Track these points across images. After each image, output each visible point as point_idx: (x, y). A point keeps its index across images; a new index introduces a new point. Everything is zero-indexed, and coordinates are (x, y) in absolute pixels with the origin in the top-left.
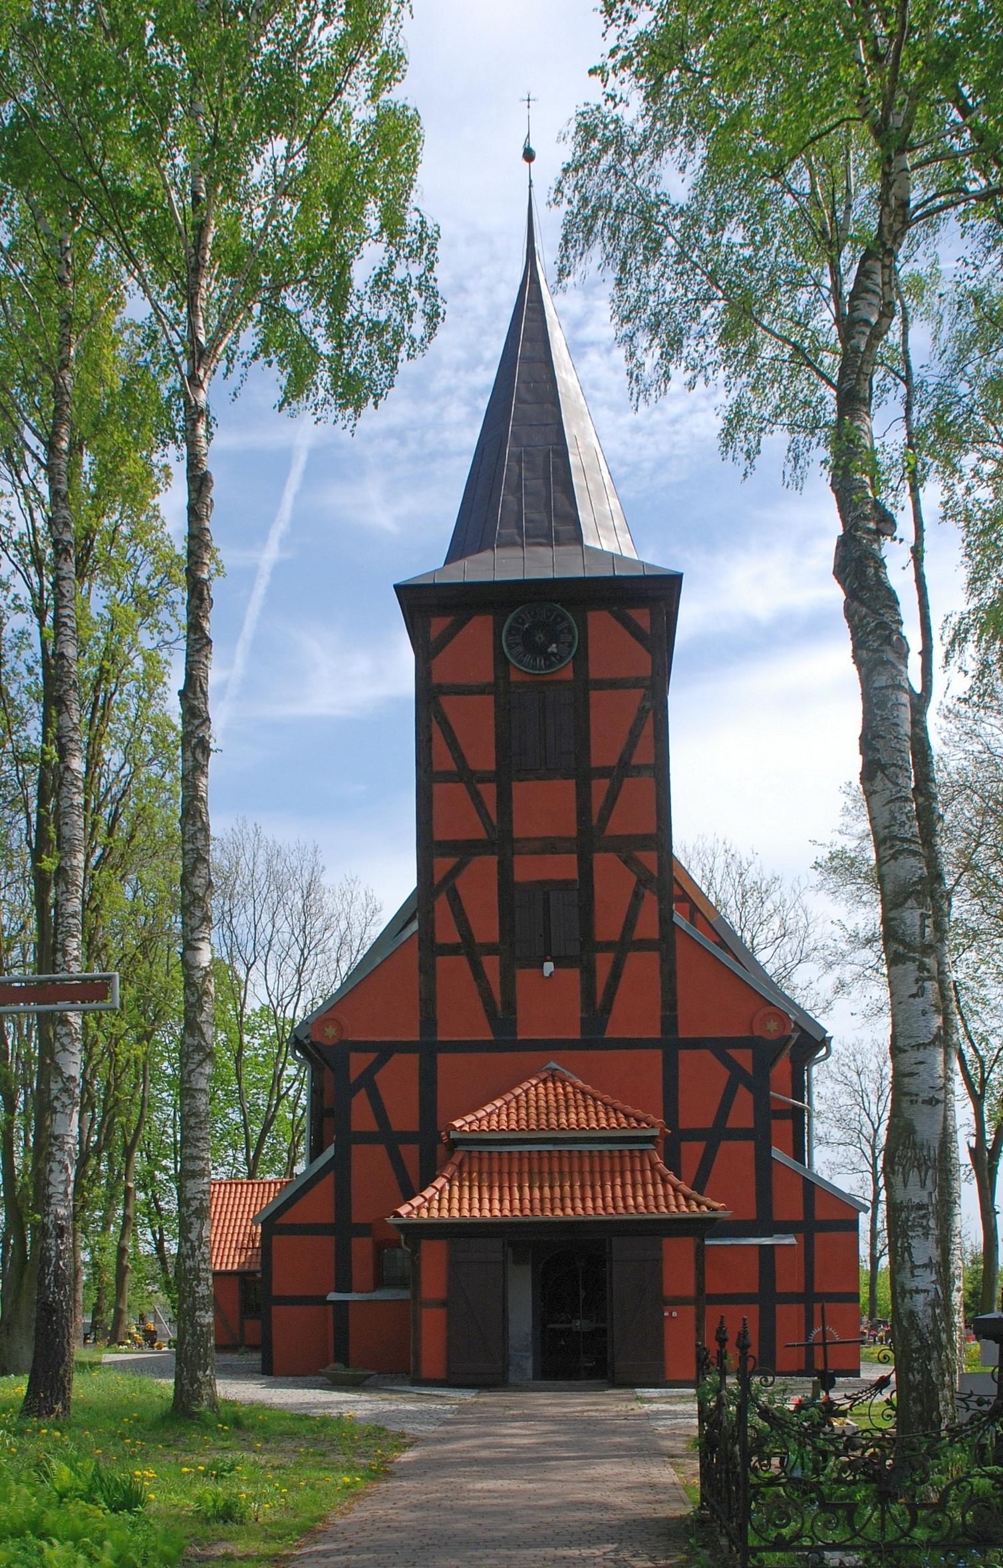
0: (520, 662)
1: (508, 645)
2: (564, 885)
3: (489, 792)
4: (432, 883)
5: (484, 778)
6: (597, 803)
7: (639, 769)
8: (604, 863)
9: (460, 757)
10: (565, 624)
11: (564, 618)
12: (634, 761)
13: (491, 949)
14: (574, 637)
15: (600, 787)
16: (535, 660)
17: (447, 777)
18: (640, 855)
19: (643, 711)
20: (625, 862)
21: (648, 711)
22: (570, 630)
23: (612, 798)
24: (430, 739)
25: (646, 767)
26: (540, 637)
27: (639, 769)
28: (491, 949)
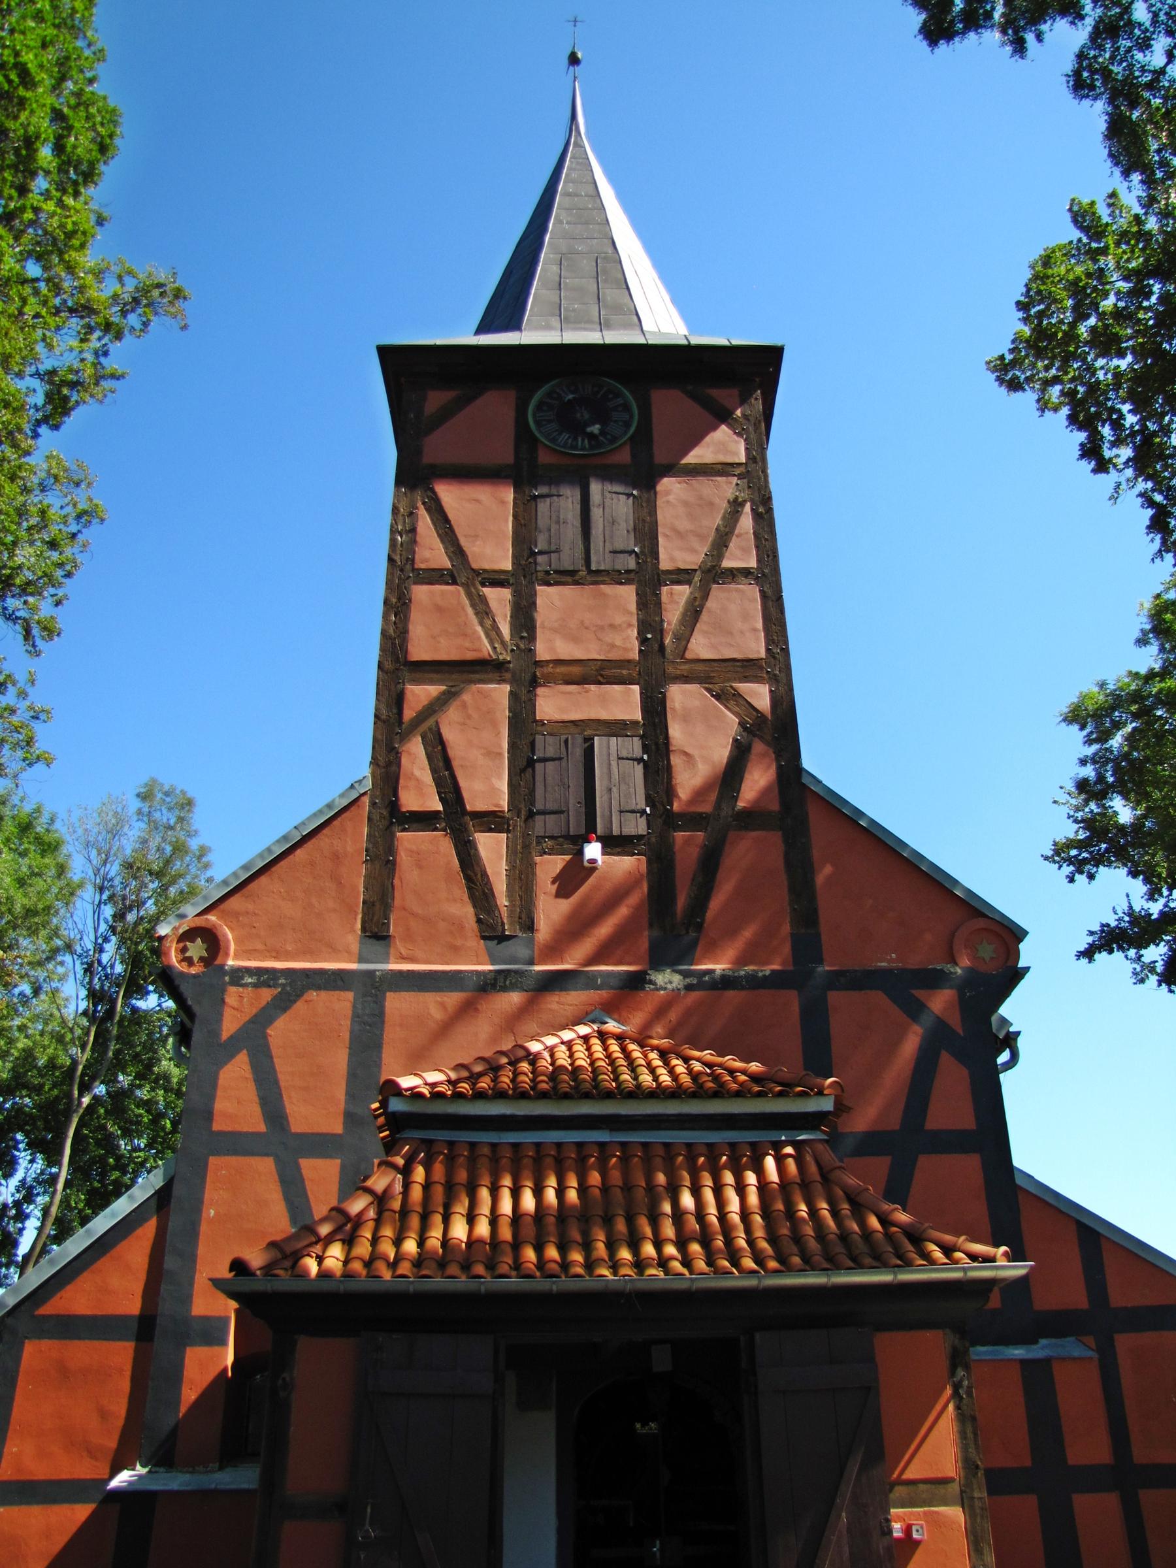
0: (553, 440)
1: (537, 422)
2: (616, 728)
3: (499, 599)
4: (400, 722)
5: (496, 580)
6: (672, 616)
7: (733, 575)
8: (680, 696)
9: (457, 551)
10: (620, 401)
11: (618, 394)
12: (727, 563)
13: (491, 821)
14: (631, 416)
15: (676, 598)
16: (575, 439)
17: (435, 576)
18: (744, 687)
19: (736, 506)
20: (717, 697)
21: (742, 504)
22: (626, 407)
23: (693, 613)
24: (413, 530)
25: (746, 572)
26: (583, 414)
27: (733, 575)
28: (491, 821)
